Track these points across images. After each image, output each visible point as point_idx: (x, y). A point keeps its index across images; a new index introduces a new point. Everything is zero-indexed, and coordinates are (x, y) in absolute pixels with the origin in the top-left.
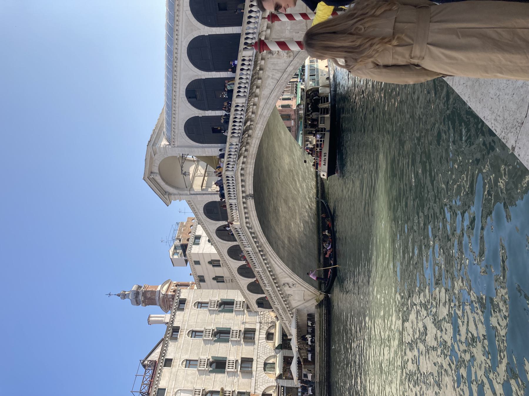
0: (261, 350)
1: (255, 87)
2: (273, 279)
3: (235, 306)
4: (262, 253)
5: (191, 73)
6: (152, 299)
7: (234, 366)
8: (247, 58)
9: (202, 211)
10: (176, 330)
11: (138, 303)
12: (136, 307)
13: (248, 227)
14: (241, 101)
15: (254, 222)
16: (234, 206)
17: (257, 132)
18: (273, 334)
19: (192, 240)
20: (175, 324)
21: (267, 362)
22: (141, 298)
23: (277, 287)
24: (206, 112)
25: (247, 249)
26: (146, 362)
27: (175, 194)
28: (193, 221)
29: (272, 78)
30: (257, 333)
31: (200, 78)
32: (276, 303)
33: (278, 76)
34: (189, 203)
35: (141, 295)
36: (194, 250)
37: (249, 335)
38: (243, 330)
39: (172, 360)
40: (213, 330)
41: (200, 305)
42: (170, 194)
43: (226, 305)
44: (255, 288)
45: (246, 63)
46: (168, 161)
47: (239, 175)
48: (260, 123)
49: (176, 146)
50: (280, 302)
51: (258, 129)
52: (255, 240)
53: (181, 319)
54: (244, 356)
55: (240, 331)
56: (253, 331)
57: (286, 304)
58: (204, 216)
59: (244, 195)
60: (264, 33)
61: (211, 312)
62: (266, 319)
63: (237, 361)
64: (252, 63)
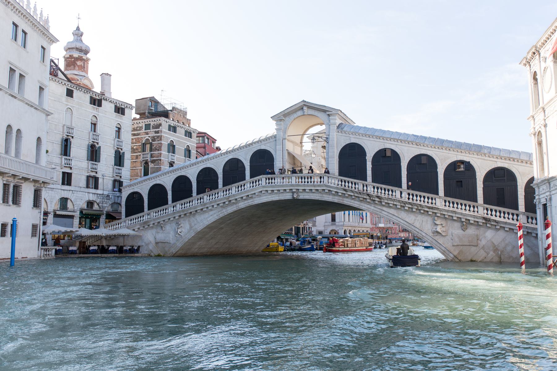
0: (80, 195)
1: (410, 206)
2: (191, 213)
3: (118, 167)
4: (227, 203)
5: (406, 155)
6: (75, 66)
7: (67, 166)
9: (263, 147)
15: (265, 197)
17: (366, 205)
19: (173, 124)
20: (103, 102)
21: (69, 201)
23: (180, 216)
24: (371, 163)
29: (415, 220)
30: (94, 191)
33: (417, 224)
35: (80, 55)
37: (93, 182)
38: (97, 176)
39: (72, 97)
40: (98, 143)
41: (119, 130)
45: (430, 201)
47: (324, 188)
48: (375, 209)
51: (369, 206)
54: (73, 175)
55: (96, 173)
56: (96, 187)
57: (154, 224)
60: (454, 215)
61: (113, 142)
62: (106, 200)
63: (71, 168)
64: (430, 205)
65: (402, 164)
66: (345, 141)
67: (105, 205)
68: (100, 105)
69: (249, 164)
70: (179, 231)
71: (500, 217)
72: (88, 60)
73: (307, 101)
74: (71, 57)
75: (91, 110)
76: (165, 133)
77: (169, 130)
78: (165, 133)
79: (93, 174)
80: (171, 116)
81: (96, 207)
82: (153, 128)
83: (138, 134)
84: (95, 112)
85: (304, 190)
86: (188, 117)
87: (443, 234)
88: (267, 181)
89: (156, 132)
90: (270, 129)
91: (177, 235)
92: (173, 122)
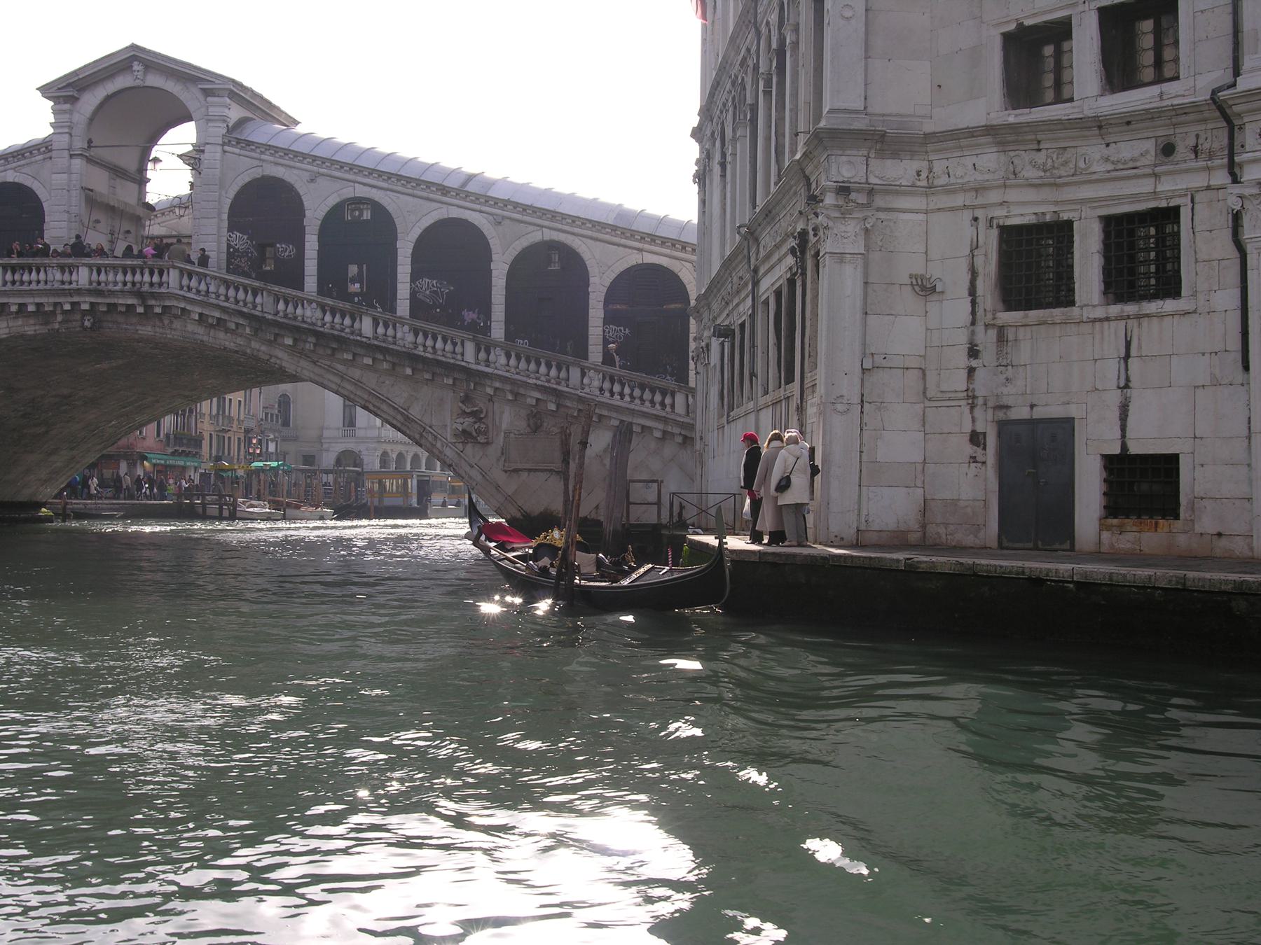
14: (366, 325)
27: (71, 112)
33: (415, 412)
42: (73, 100)
49: (226, 148)
66: (246, 170)
71: (622, 395)
85: (112, 307)
87: (481, 439)
88: (9, 277)
90: (34, 122)
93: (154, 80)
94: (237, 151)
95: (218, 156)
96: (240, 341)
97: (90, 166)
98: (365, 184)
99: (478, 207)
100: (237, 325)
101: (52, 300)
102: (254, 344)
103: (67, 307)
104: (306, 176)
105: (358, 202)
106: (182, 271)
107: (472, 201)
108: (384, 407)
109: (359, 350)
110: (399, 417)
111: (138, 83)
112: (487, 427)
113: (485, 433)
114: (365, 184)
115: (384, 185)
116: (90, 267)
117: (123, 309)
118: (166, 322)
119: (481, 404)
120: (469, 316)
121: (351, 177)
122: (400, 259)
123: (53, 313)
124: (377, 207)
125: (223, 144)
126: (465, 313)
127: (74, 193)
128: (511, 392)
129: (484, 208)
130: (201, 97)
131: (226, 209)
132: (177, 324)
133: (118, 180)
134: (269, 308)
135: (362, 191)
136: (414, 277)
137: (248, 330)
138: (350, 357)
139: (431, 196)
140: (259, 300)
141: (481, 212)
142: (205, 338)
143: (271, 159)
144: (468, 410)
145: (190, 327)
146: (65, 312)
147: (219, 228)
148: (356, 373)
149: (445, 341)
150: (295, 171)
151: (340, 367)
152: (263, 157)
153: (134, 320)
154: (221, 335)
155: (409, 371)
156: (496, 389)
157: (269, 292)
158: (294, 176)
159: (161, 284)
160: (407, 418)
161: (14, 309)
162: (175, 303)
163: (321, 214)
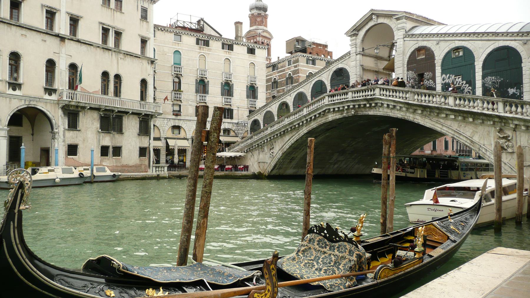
2: (277, 135)
6: (255, 23)
8: (495, 106)
9: (340, 66)
10: (231, 48)
11: (251, 9)
12: (248, 8)
13: (325, 110)
14: (451, 100)
16: (346, 97)
18: (229, 134)
22: (255, 12)
25: (305, 110)
26: (202, 23)
27: (356, 39)
28: (329, 57)
31: (476, 60)
32: (256, 137)
33: (476, 139)
34: (349, 53)
35: (259, 12)
36: (302, 58)
43: (252, 91)
44: (269, 118)
45: (490, 106)
46: (388, 32)
49: (405, 39)
50: (257, 141)
52: (313, 118)
53: (240, 51)
58: (334, 69)
59: (357, 106)
63: (206, 103)
65: (476, 63)
66: (412, 45)
67: (241, 132)
68: (232, 50)
69: (330, 84)
70: (272, 151)
72: (267, 15)
73: (374, 9)
74: (252, 14)
75: (224, 54)
76: (303, 66)
77: (307, 63)
78: (303, 66)
79: (227, 107)
80: (309, 51)
81: (232, 133)
82: (293, 64)
83: (284, 71)
84: (227, 56)
85: (359, 105)
86: (329, 49)
89: (295, 67)
91: (271, 156)
92: (310, 55)
93: (381, 20)
94: (408, 39)
95: (402, 43)
96: (402, 113)
97: (364, 57)
98: (459, 40)
99: (513, 38)
100: (401, 107)
101: (342, 105)
102: (408, 114)
103: (346, 107)
104: (435, 42)
105: (457, 49)
106: (380, 89)
107: (510, 36)
108: (461, 137)
109: (448, 112)
110: (468, 141)
111: (376, 23)
112: (513, 144)
113: (513, 147)
114: (459, 40)
115: (468, 38)
116: (352, 92)
117: (362, 106)
118: (377, 109)
119: (509, 133)
120: (511, 91)
121: (454, 38)
122: (477, 70)
123: (343, 110)
124: (464, 49)
125: (404, 38)
126: (509, 90)
127: (358, 67)
128: (524, 125)
129: (516, 38)
130: (395, 21)
131: (406, 63)
132: (381, 109)
133: (379, 61)
134: (411, 99)
135: (458, 44)
136: (484, 77)
137: (404, 109)
138: (444, 116)
139: (490, 38)
140: (407, 96)
141: (515, 40)
142: (390, 114)
143: (422, 39)
144: (501, 136)
145: (386, 110)
146: (346, 109)
147: (403, 71)
148: (449, 123)
149: (488, 103)
150: (431, 42)
151: (442, 120)
152: (418, 39)
153: (367, 110)
154: (396, 112)
155: (471, 120)
156: (516, 125)
157: (411, 92)
158: (430, 44)
159: (374, 95)
160: (472, 142)
161: (332, 110)
162: (378, 101)
163: (442, 57)
